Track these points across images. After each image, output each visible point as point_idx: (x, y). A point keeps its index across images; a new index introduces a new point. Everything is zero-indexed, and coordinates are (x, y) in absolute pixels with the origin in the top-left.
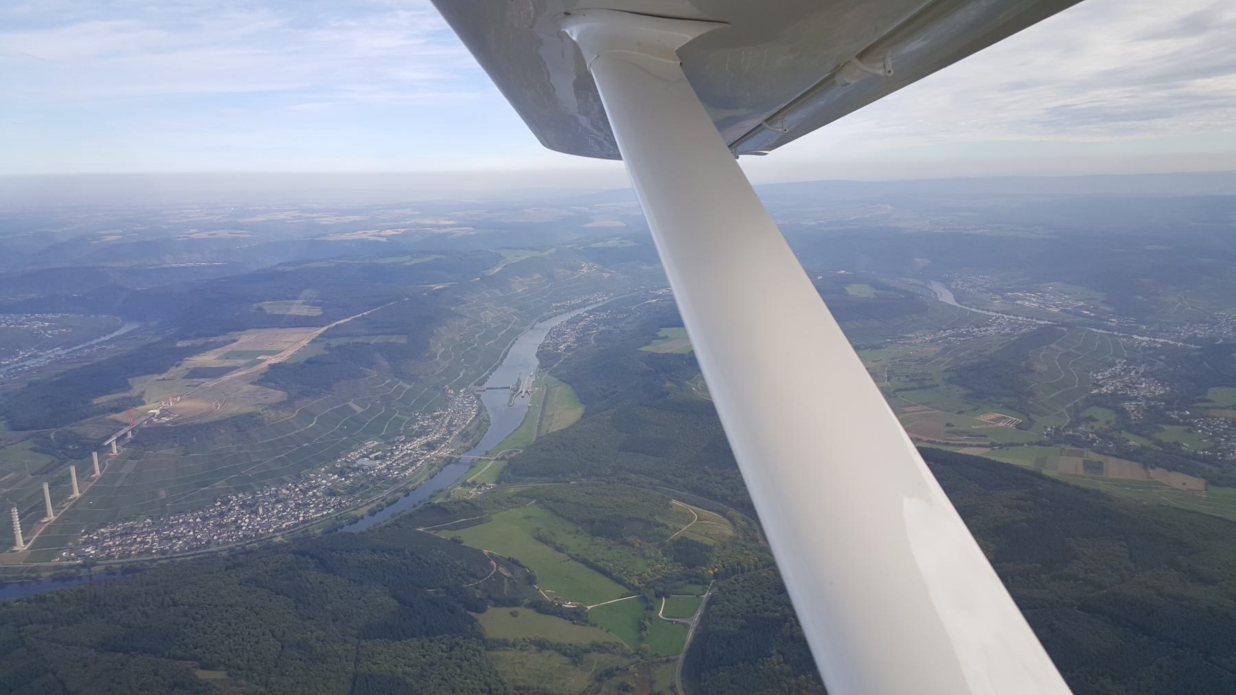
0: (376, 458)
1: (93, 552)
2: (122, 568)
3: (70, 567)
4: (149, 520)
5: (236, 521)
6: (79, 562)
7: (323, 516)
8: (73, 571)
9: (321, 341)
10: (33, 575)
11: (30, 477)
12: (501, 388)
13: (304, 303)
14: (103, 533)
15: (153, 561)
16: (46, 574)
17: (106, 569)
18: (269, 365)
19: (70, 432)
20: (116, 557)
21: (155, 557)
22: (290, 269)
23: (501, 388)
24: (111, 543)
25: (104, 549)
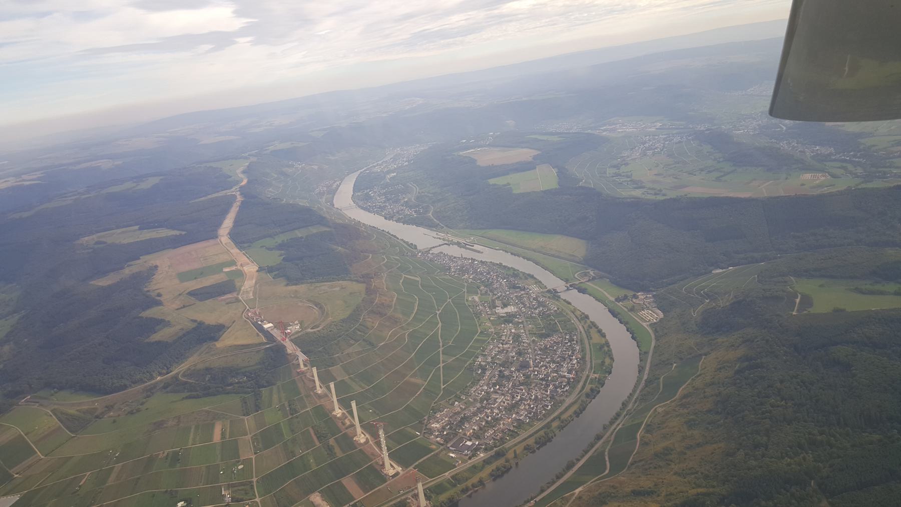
0: (505, 305)
1: (477, 443)
2: (536, 443)
3: (487, 462)
4: (456, 403)
5: (527, 377)
6: (482, 455)
7: (583, 350)
8: (501, 462)
9: (249, 246)
10: (475, 480)
11: (246, 418)
12: (440, 246)
13: (140, 229)
14: (443, 428)
15: (548, 426)
16: (484, 474)
17: (525, 449)
18: (257, 271)
19: (208, 370)
20: (508, 438)
21: (538, 425)
22: (25, 215)
23: (440, 246)
24: (471, 431)
25: (476, 436)
